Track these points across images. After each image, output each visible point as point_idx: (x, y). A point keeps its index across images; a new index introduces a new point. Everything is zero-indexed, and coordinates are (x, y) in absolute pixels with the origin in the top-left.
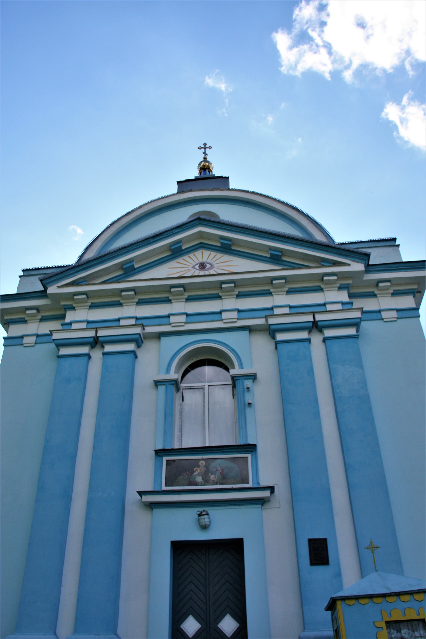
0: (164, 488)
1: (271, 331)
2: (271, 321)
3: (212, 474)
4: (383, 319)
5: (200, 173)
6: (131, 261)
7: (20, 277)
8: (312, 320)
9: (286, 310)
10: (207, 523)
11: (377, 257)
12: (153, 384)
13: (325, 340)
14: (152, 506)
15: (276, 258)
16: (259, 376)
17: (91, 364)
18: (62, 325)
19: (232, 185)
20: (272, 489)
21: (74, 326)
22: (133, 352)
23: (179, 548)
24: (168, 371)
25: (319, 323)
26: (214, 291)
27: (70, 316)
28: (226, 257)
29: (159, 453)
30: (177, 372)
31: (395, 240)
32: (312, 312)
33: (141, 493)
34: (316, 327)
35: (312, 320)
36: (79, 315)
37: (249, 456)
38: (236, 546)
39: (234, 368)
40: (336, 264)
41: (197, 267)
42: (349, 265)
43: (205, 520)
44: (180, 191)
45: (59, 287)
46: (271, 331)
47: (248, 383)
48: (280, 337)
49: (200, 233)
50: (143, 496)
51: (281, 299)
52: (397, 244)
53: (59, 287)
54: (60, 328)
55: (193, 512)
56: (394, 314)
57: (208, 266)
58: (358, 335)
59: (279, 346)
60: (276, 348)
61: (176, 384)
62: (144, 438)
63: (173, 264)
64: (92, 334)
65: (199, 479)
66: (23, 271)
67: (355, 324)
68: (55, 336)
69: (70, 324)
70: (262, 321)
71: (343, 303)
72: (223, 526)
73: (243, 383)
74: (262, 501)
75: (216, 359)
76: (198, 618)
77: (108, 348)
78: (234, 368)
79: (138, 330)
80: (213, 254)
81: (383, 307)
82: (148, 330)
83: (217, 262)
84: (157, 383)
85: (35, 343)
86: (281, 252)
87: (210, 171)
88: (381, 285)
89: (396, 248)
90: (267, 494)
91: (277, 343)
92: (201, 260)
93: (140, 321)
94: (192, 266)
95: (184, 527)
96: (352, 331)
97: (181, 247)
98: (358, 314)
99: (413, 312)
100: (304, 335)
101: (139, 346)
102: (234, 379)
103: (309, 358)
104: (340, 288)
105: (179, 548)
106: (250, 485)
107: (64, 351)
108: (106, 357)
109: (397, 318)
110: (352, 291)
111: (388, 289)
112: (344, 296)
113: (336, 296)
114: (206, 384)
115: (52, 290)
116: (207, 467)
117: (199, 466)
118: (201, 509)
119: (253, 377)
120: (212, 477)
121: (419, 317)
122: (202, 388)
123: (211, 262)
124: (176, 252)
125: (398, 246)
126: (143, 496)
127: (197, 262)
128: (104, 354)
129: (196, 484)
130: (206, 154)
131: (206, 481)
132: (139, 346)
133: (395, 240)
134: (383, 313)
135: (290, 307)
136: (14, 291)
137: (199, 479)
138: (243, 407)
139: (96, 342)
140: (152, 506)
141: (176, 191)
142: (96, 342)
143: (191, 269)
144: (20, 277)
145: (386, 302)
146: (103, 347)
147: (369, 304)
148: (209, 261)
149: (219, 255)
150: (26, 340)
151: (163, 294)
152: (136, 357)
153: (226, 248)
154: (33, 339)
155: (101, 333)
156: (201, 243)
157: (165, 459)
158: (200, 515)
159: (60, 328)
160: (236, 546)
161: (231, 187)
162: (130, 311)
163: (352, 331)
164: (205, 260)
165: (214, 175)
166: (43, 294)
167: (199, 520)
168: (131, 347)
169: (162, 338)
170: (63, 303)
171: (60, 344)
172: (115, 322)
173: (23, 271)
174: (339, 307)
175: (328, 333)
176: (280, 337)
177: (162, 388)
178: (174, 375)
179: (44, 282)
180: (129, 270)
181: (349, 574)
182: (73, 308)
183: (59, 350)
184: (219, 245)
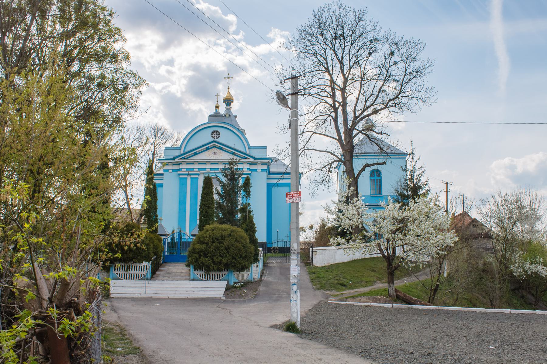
15: (233, 154)
27: (181, 166)
28: (221, 151)
40: (247, 158)
44: (210, 122)
63: (207, 152)
68: (179, 173)
79: (199, 173)
82: (201, 172)
107: (181, 176)
112: (248, 166)
124: (208, 149)
153: (221, 149)
162: (196, 166)
171: (180, 175)
180: (196, 154)
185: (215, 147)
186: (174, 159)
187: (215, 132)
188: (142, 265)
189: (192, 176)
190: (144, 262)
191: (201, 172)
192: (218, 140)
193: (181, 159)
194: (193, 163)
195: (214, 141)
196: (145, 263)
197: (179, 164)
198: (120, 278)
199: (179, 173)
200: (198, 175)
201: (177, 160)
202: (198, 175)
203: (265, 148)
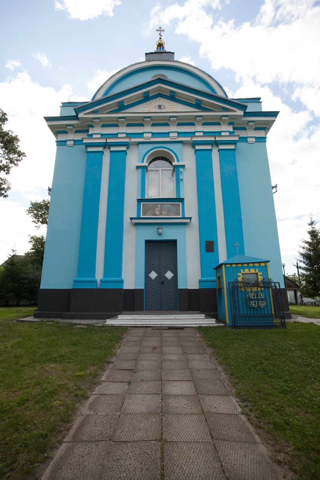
0: (141, 216)
1: (193, 144)
2: (194, 139)
3: (163, 211)
4: (248, 142)
5: (158, 48)
6: (123, 101)
7: (61, 107)
8: (214, 140)
9: (202, 134)
10: (162, 232)
11: (251, 108)
12: (135, 168)
13: (219, 150)
14: (136, 224)
15: (198, 105)
16: (186, 166)
17: (104, 157)
18: (88, 135)
19: (176, 58)
20: (190, 218)
22: (125, 151)
23: (148, 243)
24: (143, 162)
25: (217, 142)
26: (165, 122)
29: (139, 201)
30: (147, 162)
31: (260, 99)
32: (214, 136)
33: (131, 219)
34: (216, 143)
35: (214, 140)
36: (97, 131)
37: (181, 203)
38: (174, 243)
39: (174, 161)
41: (157, 107)
42: (236, 111)
43: (161, 231)
44: (147, 61)
45: (85, 114)
46: (193, 144)
47: (181, 169)
48: (198, 147)
50: (132, 220)
51: (199, 128)
52: (260, 101)
53: (85, 114)
54: (87, 137)
55: (157, 227)
56: (254, 140)
57: (163, 107)
58: (236, 149)
59: (196, 152)
60: (195, 153)
61: (145, 168)
62: (131, 194)
63: (144, 105)
64: (104, 141)
65: (158, 213)
66: (62, 103)
67: (234, 143)
68: (85, 141)
69: (92, 135)
70: (189, 139)
71: (230, 132)
72: (168, 234)
73: (179, 169)
74: (185, 224)
75: (167, 158)
76: (156, 272)
77: (113, 149)
78: (174, 161)
80: (166, 100)
81: (248, 136)
82: (133, 140)
83: (167, 105)
84: (138, 167)
85: (73, 145)
86: (201, 101)
87: (163, 48)
88: (250, 123)
89: (260, 103)
90: (188, 221)
91: (196, 150)
92: (159, 104)
93: (129, 135)
94: (154, 106)
95: (151, 234)
96: (233, 147)
97: (149, 95)
98: (237, 139)
99: (263, 140)
100: (209, 147)
101: (128, 148)
102: (175, 167)
103: (210, 159)
104: (230, 124)
105: (148, 243)
106: (181, 216)
107: (89, 149)
108: (112, 153)
109: (255, 142)
110: (235, 126)
111: (253, 126)
113: (226, 128)
114: (161, 169)
115: (81, 115)
116: (161, 207)
117: (157, 207)
118: (159, 226)
119: (183, 166)
120: (164, 212)
121: (266, 142)
122: (158, 171)
123: (164, 105)
124: (147, 98)
125: (261, 102)
126: (132, 220)
127: (157, 104)
128: (111, 152)
129: (156, 215)
130: (161, 36)
131: (161, 214)
132: (128, 148)
133: (260, 99)
134: (248, 139)
135: (204, 132)
136: (58, 114)
137: (158, 213)
138: (178, 182)
139: (106, 145)
140: (136, 224)
141: (144, 60)
142: (106, 145)
143: (154, 108)
144: (61, 107)
145: (251, 134)
146: (110, 148)
147: (243, 134)
148: (163, 104)
149: (169, 101)
150: (68, 143)
151: (139, 122)
152: (127, 154)
153: (173, 97)
154: (72, 143)
155: (108, 141)
156: (160, 93)
157: (142, 203)
158: (158, 229)
159: (87, 137)
160: (174, 243)
161: (175, 59)
162: (123, 130)
163: (233, 147)
164: (161, 104)
165: (166, 51)
166: (76, 118)
167: (158, 231)
168: (124, 148)
169: (139, 145)
170: (87, 123)
171: (88, 145)
172: (116, 135)
173: (62, 103)
174: (228, 134)
175: (221, 147)
176: (198, 147)
177: (140, 170)
178: (145, 164)
179: (76, 110)
180: (121, 107)
181: (223, 258)
182: (93, 126)
183: (87, 149)
184: (169, 95)
185: (160, 95)
186: (76, 118)
191: (133, 140)
200: (127, 145)
203: (257, 100)
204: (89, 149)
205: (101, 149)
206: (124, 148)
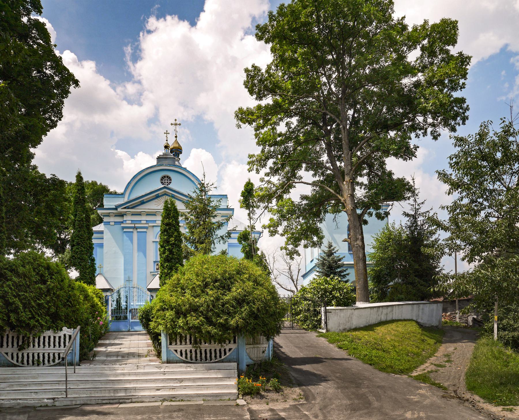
21: (127, 222)
22: (146, 232)
27: (125, 218)
49: (165, 191)
63: (156, 200)
68: (122, 225)
82: (150, 224)
84: (153, 242)
107: (125, 230)
124: (157, 197)
139: (135, 228)
150: (111, 223)
154: (113, 223)
162: (144, 218)
171: (123, 228)
177: (155, 243)
180: (143, 203)
185: (166, 194)
186: (116, 209)
187: (165, 177)
188: (61, 334)
189: (139, 230)
190: (64, 328)
192: (170, 186)
193: (125, 208)
194: (139, 214)
195: (165, 187)
196: (66, 331)
197: (122, 215)
198: (15, 362)
199: (122, 225)
200: (146, 228)
201: (119, 210)
202: (146, 228)
204: (125, 230)
205: (131, 230)
206: (145, 230)
